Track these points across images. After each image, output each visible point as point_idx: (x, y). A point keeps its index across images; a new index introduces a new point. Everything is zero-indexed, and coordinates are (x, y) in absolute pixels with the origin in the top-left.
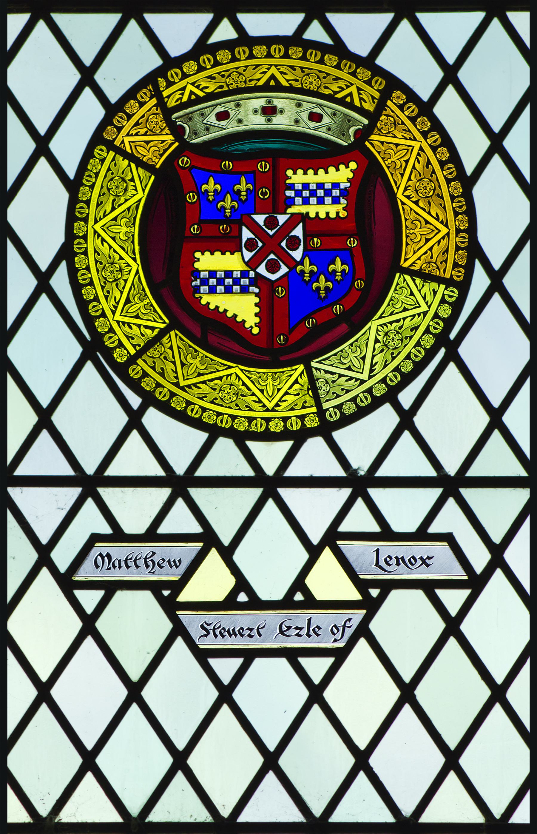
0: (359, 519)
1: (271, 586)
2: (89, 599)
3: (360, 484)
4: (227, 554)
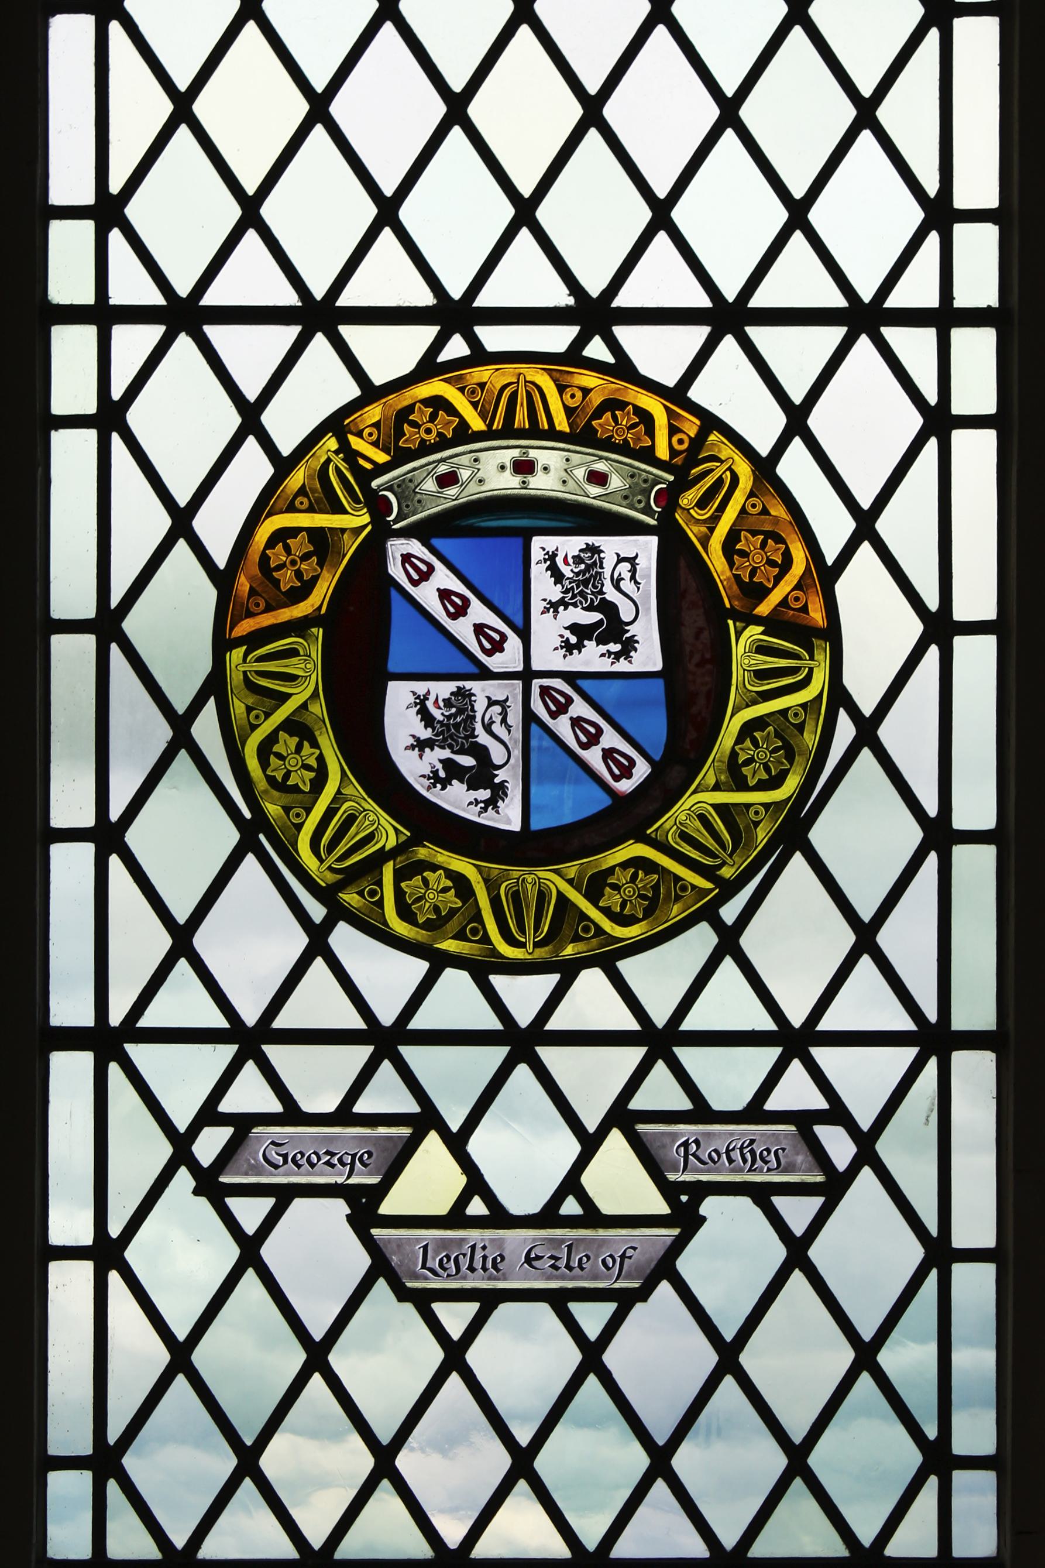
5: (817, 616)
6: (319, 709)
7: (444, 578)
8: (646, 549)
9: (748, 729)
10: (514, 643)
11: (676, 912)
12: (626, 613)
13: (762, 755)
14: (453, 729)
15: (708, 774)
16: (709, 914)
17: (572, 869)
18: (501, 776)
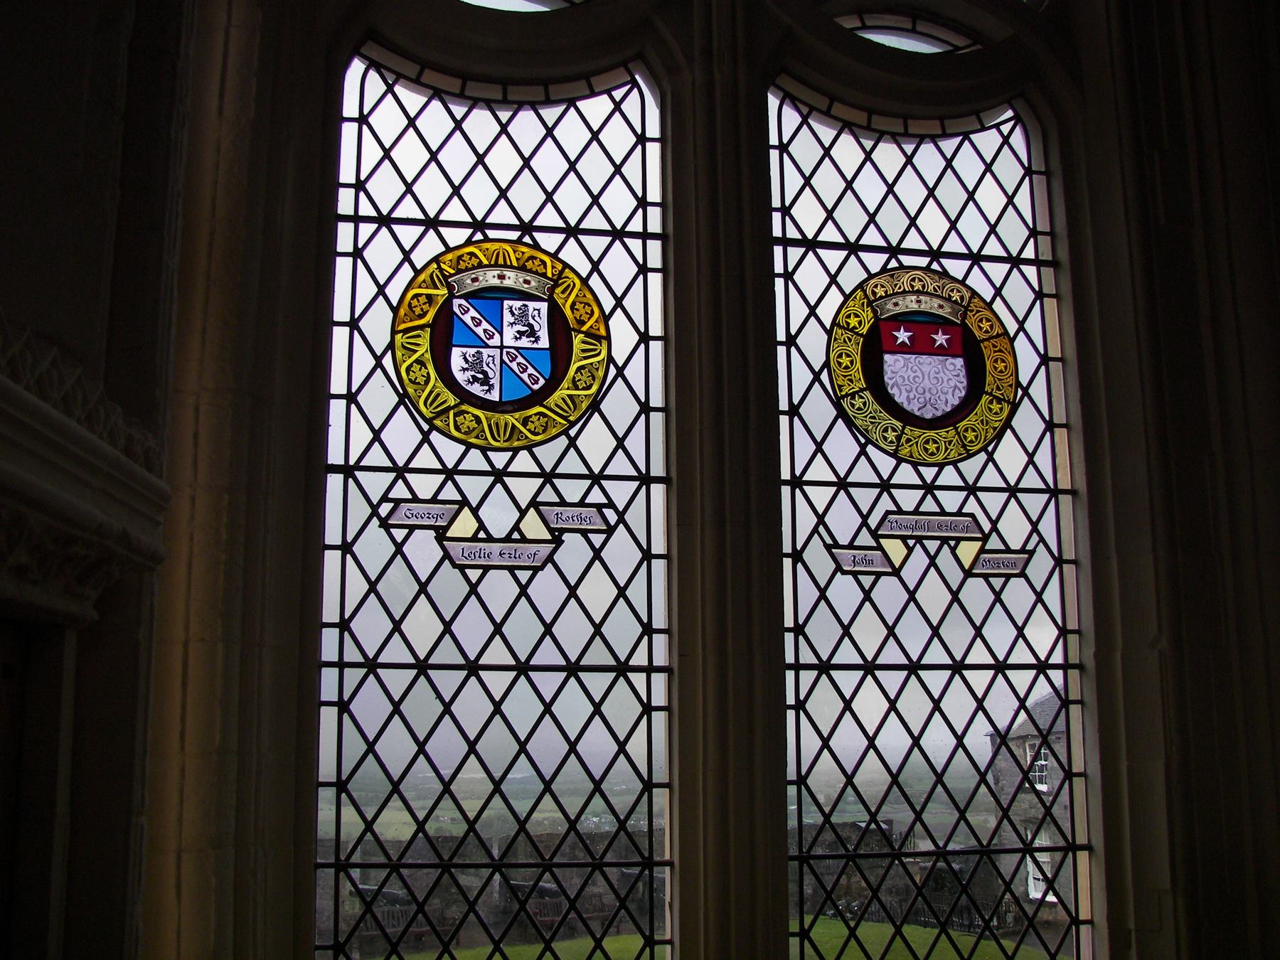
0: (548, 495)
1: (499, 528)
2: (399, 534)
3: (548, 477)
4: (475, 512)
5: (603, 332)
6: (428, 356)
7: (473, 313)
8: (544, 306)
9: (579, 369)
10: (497, 336)
11: (554, 432)
12: (537, 328)
13: (584, 378)
14: (475, 364)
15: (565, 384)
16: (565, 432)
17: (517, 415)
18: (492, 382)
